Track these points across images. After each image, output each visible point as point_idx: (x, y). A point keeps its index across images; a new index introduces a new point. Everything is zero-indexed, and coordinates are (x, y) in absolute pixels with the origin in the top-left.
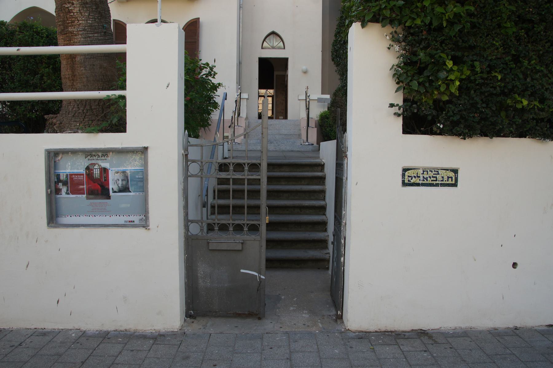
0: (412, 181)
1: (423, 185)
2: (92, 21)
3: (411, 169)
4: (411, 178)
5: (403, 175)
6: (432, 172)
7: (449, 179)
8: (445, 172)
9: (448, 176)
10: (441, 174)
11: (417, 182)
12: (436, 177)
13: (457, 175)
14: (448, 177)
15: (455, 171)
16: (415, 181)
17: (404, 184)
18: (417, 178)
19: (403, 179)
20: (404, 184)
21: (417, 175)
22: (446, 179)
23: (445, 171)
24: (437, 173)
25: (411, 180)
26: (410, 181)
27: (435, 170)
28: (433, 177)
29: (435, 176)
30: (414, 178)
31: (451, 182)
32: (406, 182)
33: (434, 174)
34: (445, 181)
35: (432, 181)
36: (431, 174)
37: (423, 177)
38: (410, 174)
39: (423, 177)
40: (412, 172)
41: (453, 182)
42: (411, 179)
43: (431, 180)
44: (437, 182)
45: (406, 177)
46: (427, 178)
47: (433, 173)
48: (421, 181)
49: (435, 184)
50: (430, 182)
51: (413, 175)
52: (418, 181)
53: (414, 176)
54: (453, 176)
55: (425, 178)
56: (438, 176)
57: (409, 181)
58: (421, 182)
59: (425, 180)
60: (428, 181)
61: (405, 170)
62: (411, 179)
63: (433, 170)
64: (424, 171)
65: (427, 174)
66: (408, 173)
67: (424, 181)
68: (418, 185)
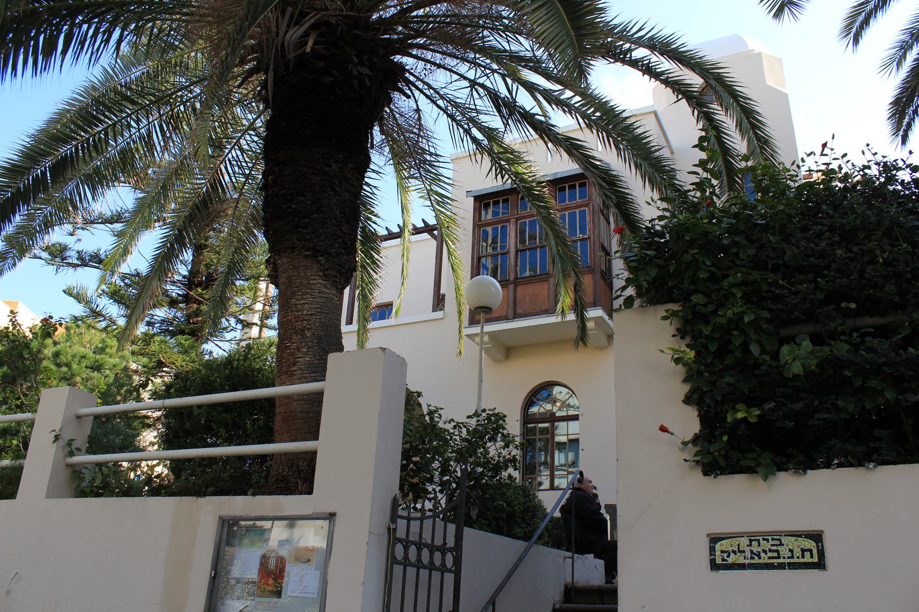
0: (730, 560)
2: (310, 358)
3: (726, 538)
4: (727, 554)
5: (712, 550)
6: (768, 542)
7: (806, 553)
9: (801, 547)
10: (787, 545)
12: (778, 551)
13: (822, 546)
14: (803, 551)
15: (817, 537)
16: (736, 561)
17: (714, 566)
18: (739, 554)
19: (712, 557)
20: (714, 566)
21: (739, 548)
22: (800, 554)
23: (794, 538)
24: (778, 543)
25: (728, 559)
26: (726, 560)
27: (775, 537)
28: (770, 551)
29: (775, 548)
30: (732, 555)
31: (810, 560)
32: (717, 562)
33: (772, 545)
35: (770, 558)
36: (766, 545)
37: (752, 552)
38: (725, 547)
39: (752, 552)
41: (816, 559)
42: (728, 556)
44: (781, 560)
45: (718, 553)
46: (759, 552)
47: (771, 542)
48: (748, 559)
49: (776, 564)
50: (765, 559)
51: (730, 549)
52: (741, 560)
54: (814, 547)
55: (755, 554)
56: (779, 548)
57: (723, 560)
59: (756, 557)
61: (714, 540)
62: (728, 556)
63: (770, 538)
64: (751, 541)
65: (759, 545)
66: (722, 545)
67: (754, 558)
68: (742, 567)
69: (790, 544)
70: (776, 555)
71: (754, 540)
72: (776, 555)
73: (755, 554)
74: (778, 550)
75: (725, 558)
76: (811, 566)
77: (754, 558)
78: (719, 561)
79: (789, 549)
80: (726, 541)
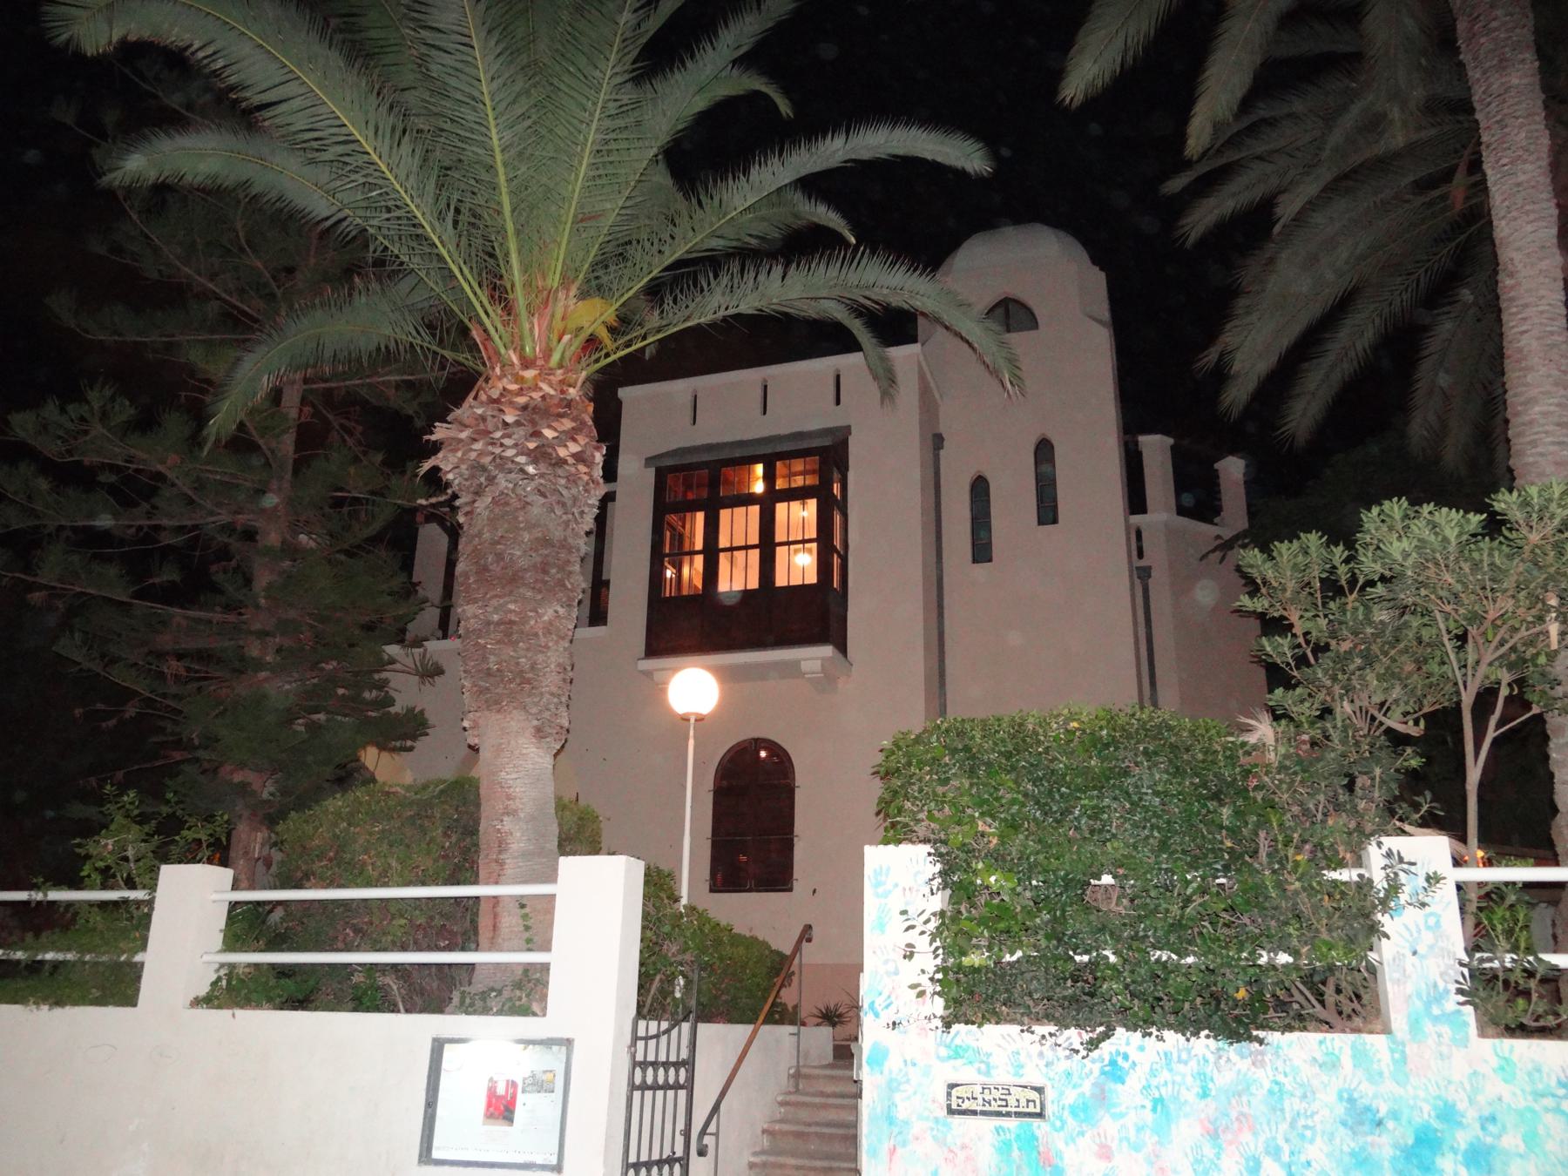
1: (984, 1113)
5: (949, 1094)
14: (1028, 1101)
15: (1040, 1090)
20: (951, 1112)
36: (997, 1094)
44: (1009, 1109)
50: (994, 1107)
52: (974, 1107)
58: (979, 1108)
68: (974, 1113)
78: (954, 1107)
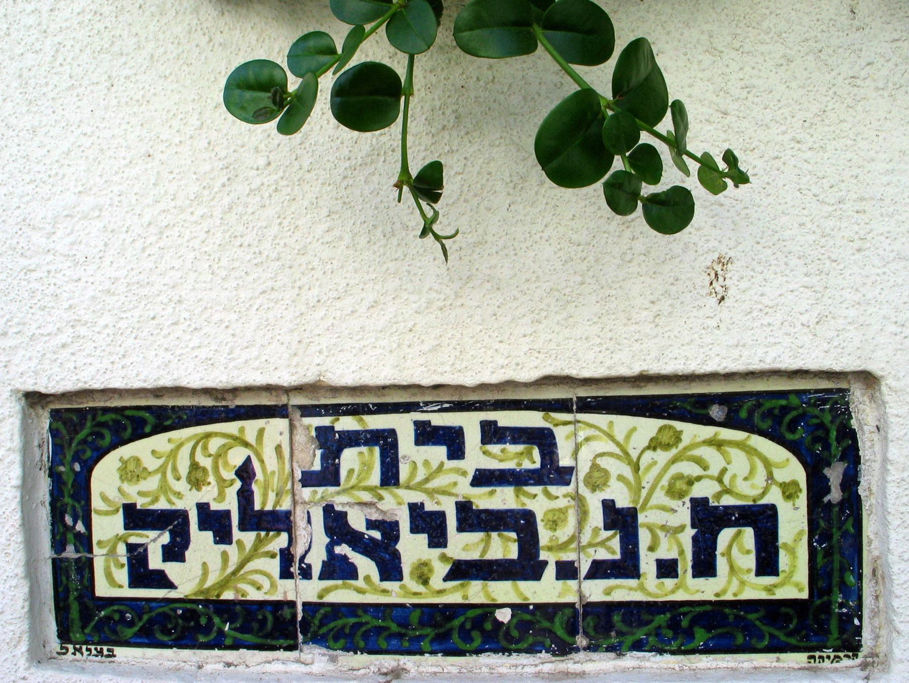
4: (166, 538)
6: (456, 451)
7: (725, 536)
8: (654, 445)
9: (700, 490)
11: (254, 595)
13: (851, 481)
16: (224, 584)
18: (249, 538)
21: (245, 496)
23: (648, 427)
24: (533, 460)
25: (172, 570)
26: (161, 580)
27: (506, 419)
32: (102, 589)
33: (483, 478)
34: (667, 569)
38: (151, 484)
40: (173, 454)
43: (442, 569)
46: (390, 529)
48: (306, 573)
49: (504, 616)
53: (202, 508)
54: (789, 491)
55: (356, 540)
59: (366, 566)
60: (408, 581)
65: (390, 477)
67: (349, 572)
69: (615, 467)
70: (513, 553)
71: (352, 439)
72: (513, 553)
73: (356, 540)
74: (529, 516)
75: (155, 561)
76: (749, 629)
77: (349, 572)
79: (608, 506)
80: (160, 442)
